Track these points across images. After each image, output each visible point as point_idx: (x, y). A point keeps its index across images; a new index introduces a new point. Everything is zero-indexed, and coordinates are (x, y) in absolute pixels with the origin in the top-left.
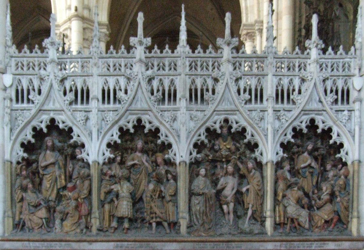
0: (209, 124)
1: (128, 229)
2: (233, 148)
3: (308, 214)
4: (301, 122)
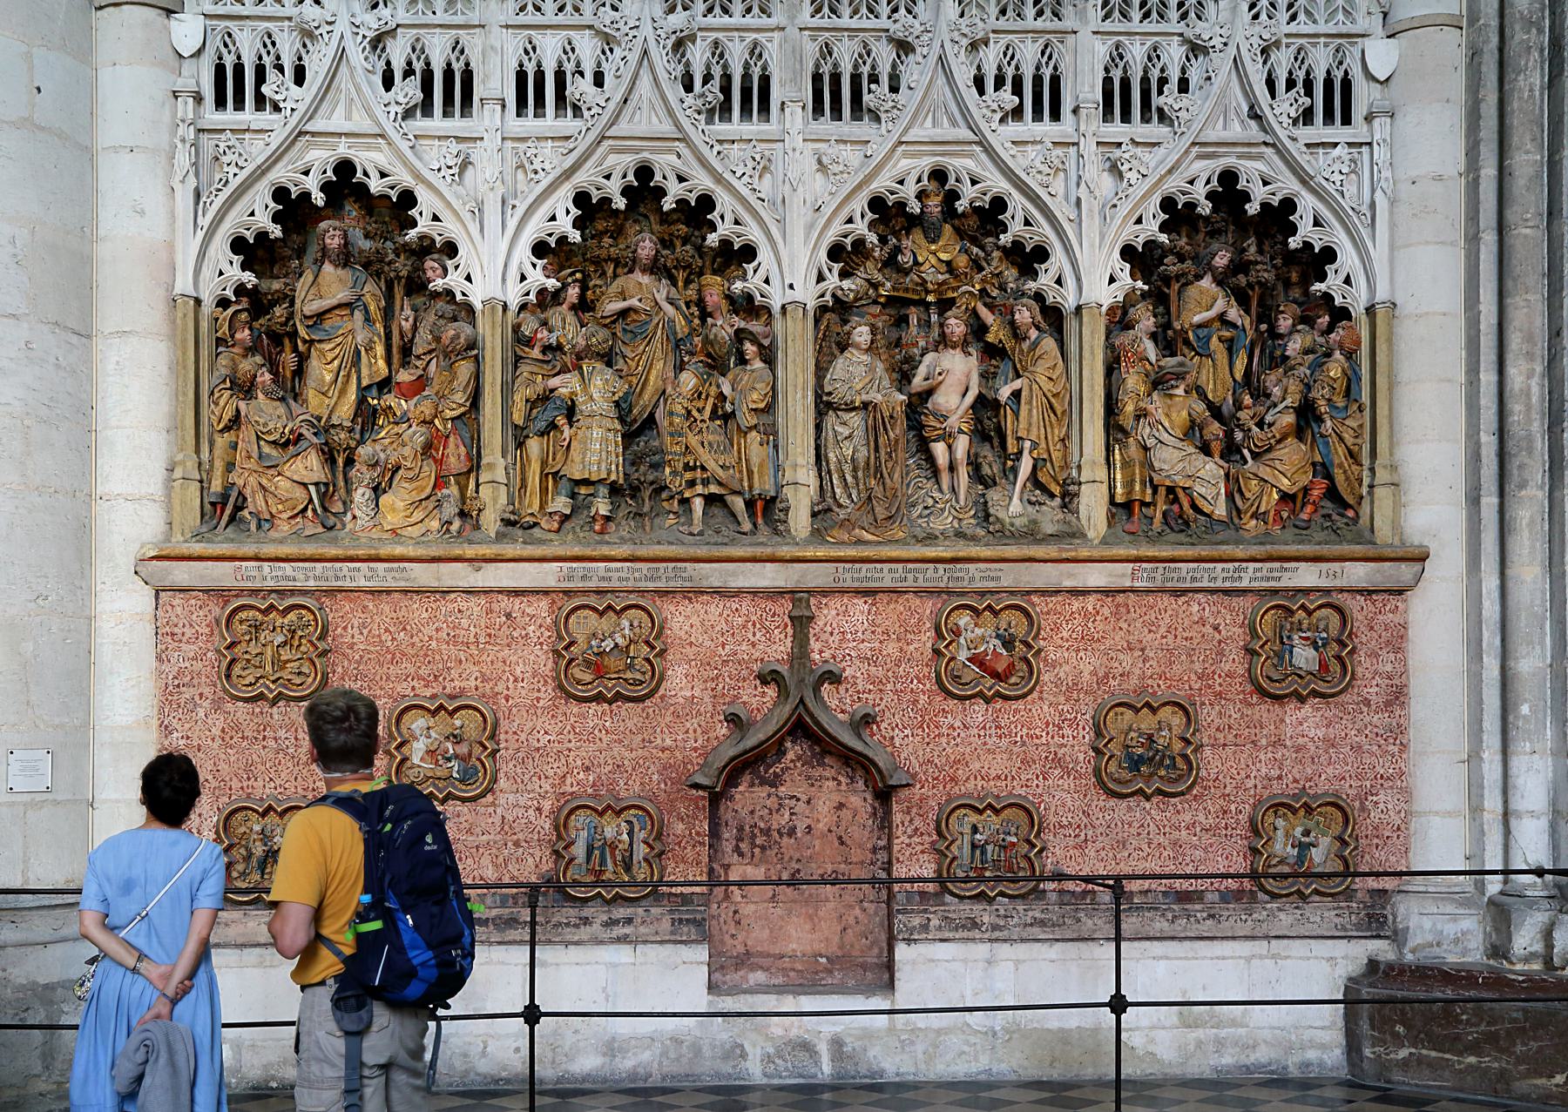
0: (882, 184)
1: (608, 519)
2: (962, 262)
3: (1222, 472)
4: (1191, 182)
